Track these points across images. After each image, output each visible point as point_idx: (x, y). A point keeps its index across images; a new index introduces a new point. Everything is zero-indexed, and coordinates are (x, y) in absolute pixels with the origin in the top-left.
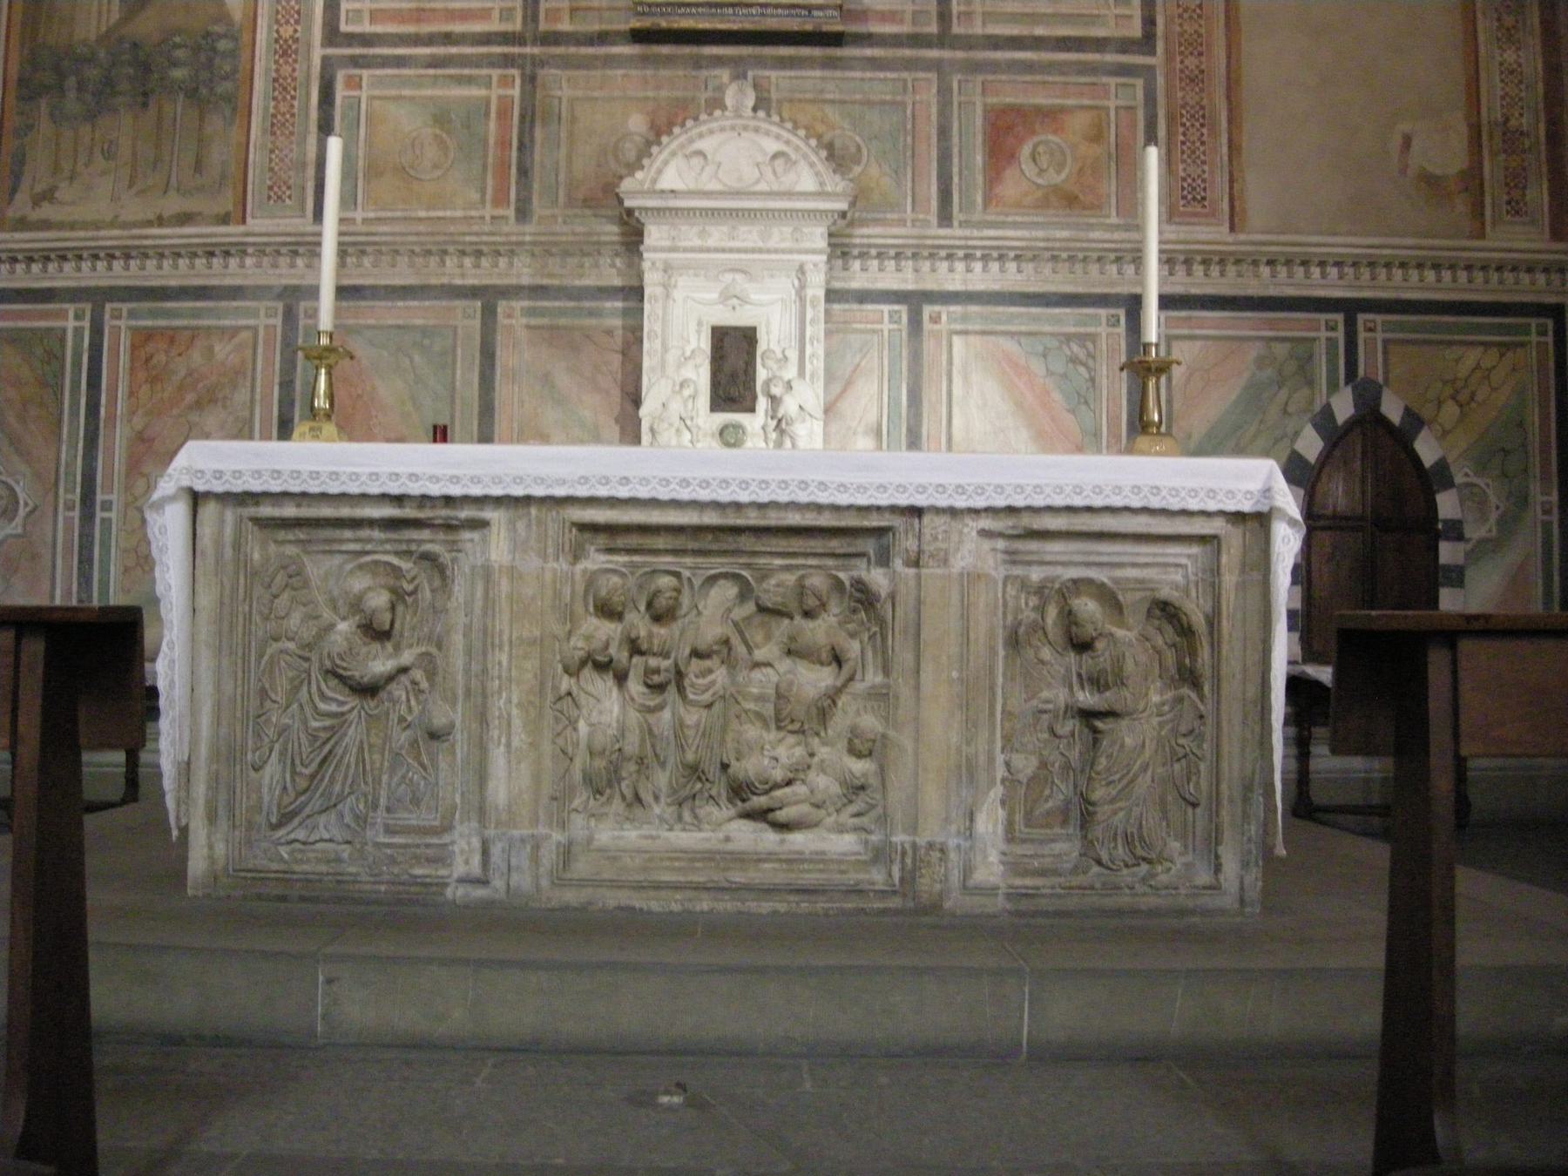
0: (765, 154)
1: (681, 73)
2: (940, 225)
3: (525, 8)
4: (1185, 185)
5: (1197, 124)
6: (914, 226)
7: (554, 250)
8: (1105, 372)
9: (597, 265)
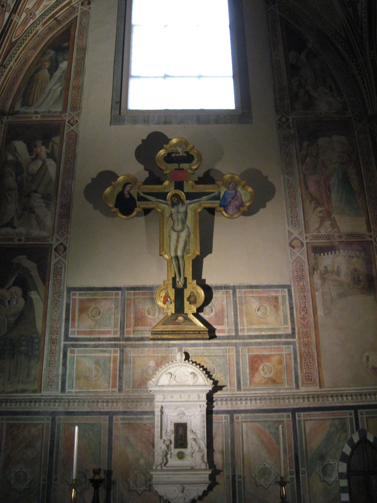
1: (164, 349)
2: (238, 391)
3: (121, 330)
4: (306, 375)
5: (308, 358)
7: (129, 400)
8: (286, 432)
9: (141, 405)
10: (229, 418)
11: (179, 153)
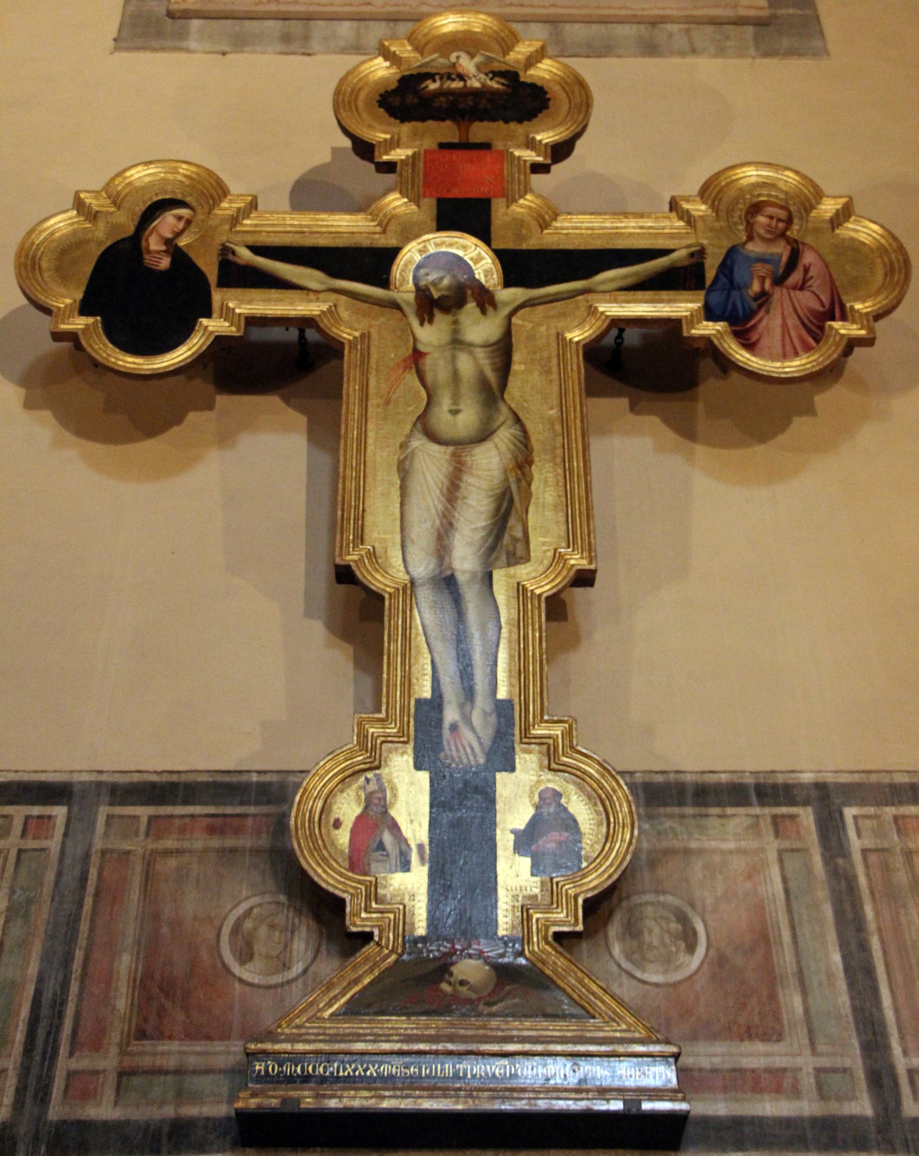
11: (461, 77)
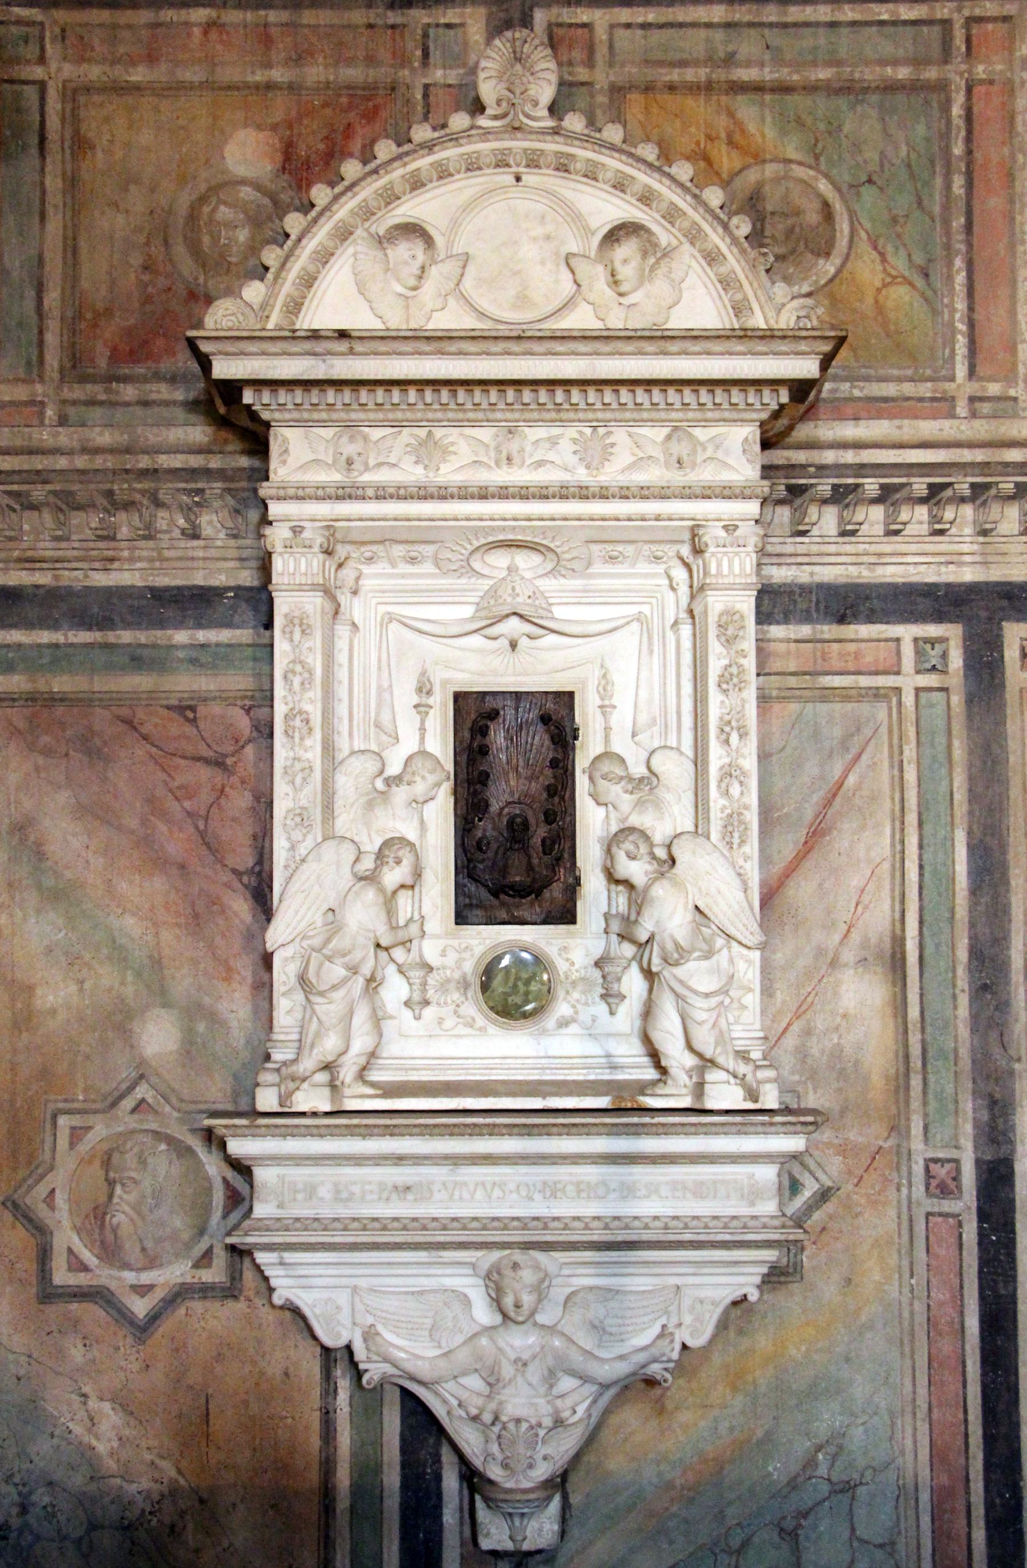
0: (588, 232)
6: (974, 415)
7: (38, 493)
9: (150, 534)
10: (956, 660)
